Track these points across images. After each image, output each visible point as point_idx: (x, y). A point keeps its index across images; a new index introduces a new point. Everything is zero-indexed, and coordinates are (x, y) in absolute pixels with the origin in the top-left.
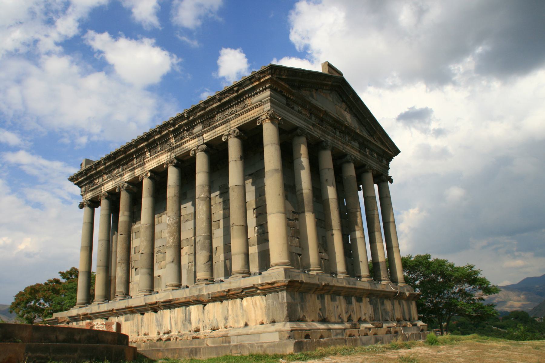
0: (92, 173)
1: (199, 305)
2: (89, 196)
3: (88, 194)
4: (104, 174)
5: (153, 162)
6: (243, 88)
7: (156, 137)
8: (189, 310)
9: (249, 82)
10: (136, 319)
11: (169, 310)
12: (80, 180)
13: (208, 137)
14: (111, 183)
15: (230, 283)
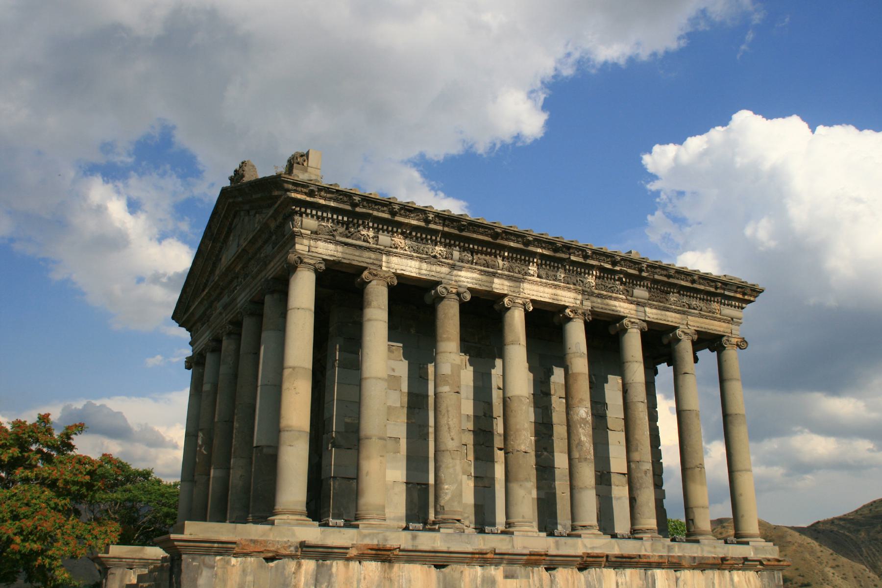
0: (375, 213)
1: (669, 570)
2: (327, 250)
3: (320, 244)
4: (402, 233)
5: (541, 289)
6: (724, 289)
7: (573, 258)
8: (653, 576)
9: (734, 288)
10: (536, 578)
11: (612, 570)
12: (322, 202)
13: (652, 314)
14: (414, 264)
15: (715, 547)
